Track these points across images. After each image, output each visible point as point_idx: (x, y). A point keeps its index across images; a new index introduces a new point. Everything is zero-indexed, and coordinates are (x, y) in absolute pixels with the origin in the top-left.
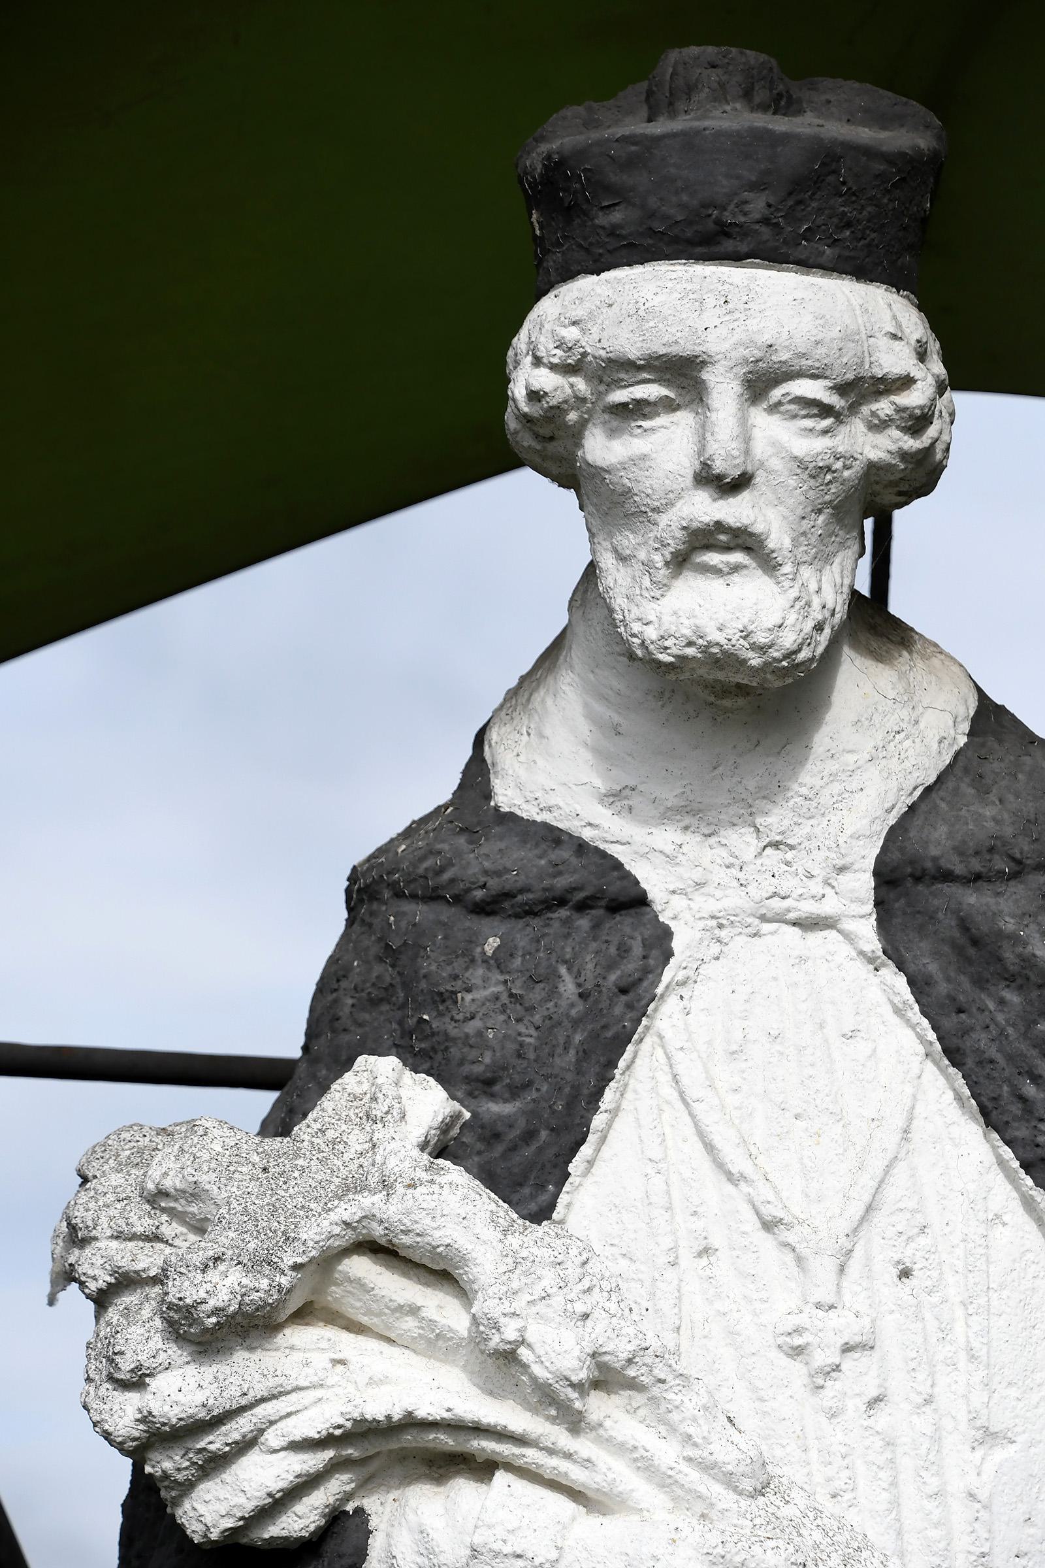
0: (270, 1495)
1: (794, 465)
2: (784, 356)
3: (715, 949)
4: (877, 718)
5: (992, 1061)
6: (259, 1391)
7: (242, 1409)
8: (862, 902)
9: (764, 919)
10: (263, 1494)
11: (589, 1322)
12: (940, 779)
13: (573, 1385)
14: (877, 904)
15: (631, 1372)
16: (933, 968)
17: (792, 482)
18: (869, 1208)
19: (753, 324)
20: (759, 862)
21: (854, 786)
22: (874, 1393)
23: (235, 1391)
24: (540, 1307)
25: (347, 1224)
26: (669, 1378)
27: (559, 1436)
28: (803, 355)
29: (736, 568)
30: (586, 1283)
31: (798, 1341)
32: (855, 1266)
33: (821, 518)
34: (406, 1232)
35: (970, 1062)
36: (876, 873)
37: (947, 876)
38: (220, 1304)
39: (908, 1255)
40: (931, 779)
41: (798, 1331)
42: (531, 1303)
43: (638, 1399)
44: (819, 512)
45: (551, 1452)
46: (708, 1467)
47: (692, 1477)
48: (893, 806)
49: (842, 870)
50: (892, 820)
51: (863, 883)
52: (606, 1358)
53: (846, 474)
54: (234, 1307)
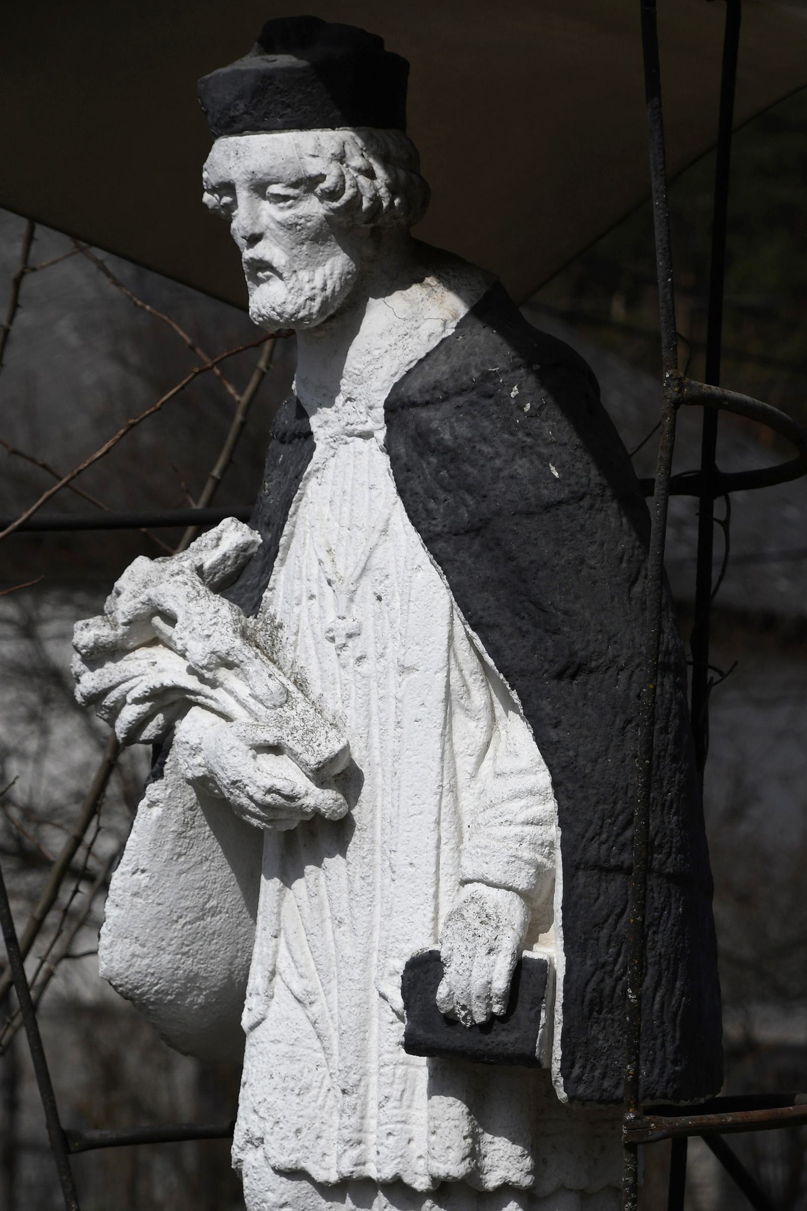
0: (130, 723)
1: (279, 225)
2: (260, 176)
3: (332, 452)
4: (394, 330)
5: (417, 494)
6: (117, 679)
7: (112, 688)
8: (378, 422)
9: (350, 435)
10: (126, 723)
11: (211, 638)
12: (428, 355)
13: (202, 668)
14: (386, 422)
15: (230, 659)
16: (402, 450)
17: (281, 233)
18: (364, 570)
19: (246, 163)
20: (343, 408)
21: (378, 366)
22: (359, 655)
23: (106, 681)
24: (193, 634)
25: (143, 603)
26: (245, 660)
27: (207, 689)
28: (267, 174)
29: (269, 278)
30: (214, 621)
31: (331, 635)
32: (357, 598)
33: (304, 248)
34: (158, 605)
35: (407, 495)
36: (385, 407)
37: (414, 404)
38: (85, 644)
39: (380, 589)
40: (423, 355)
41: (331, 630)
42: (190, 632)
43: (239, 670)
44: (302, 244)
45: (206, 697)
46: (255, 697)
47: (251, 701)
48: (396, 373)
49: (371, 408)
50: (396, 379)
51: (380, 412)
52: (219, 654)
53: (309, 224)
54: (91, 644)
